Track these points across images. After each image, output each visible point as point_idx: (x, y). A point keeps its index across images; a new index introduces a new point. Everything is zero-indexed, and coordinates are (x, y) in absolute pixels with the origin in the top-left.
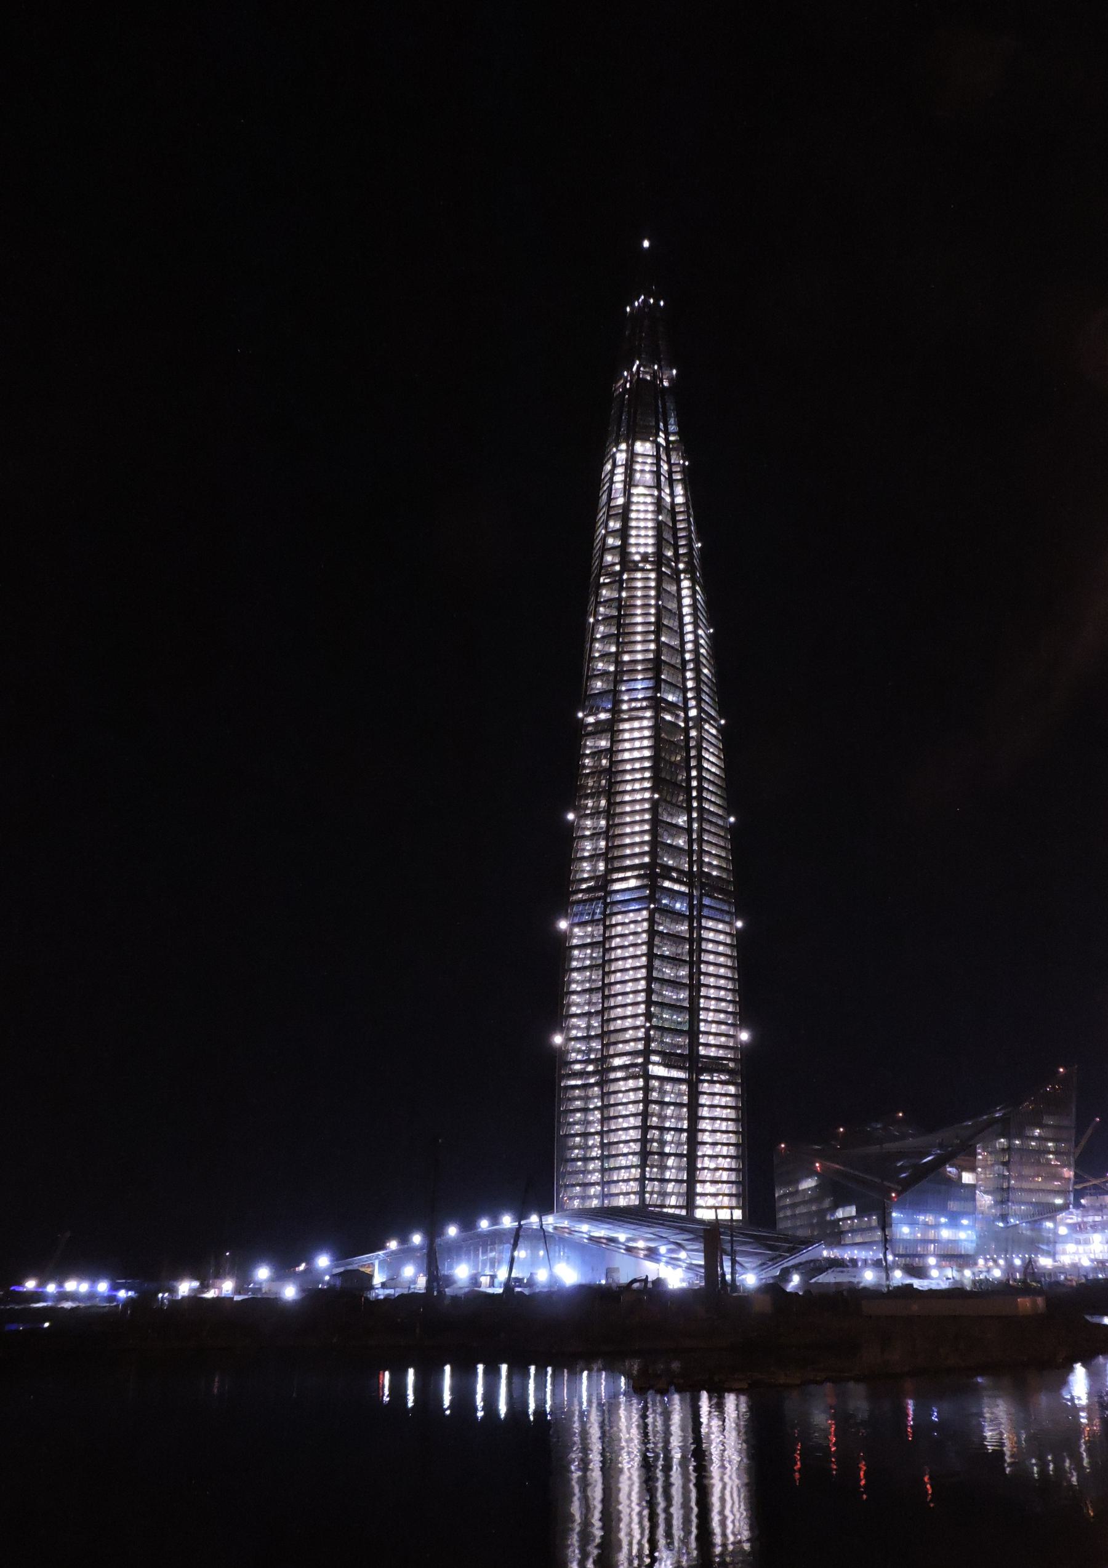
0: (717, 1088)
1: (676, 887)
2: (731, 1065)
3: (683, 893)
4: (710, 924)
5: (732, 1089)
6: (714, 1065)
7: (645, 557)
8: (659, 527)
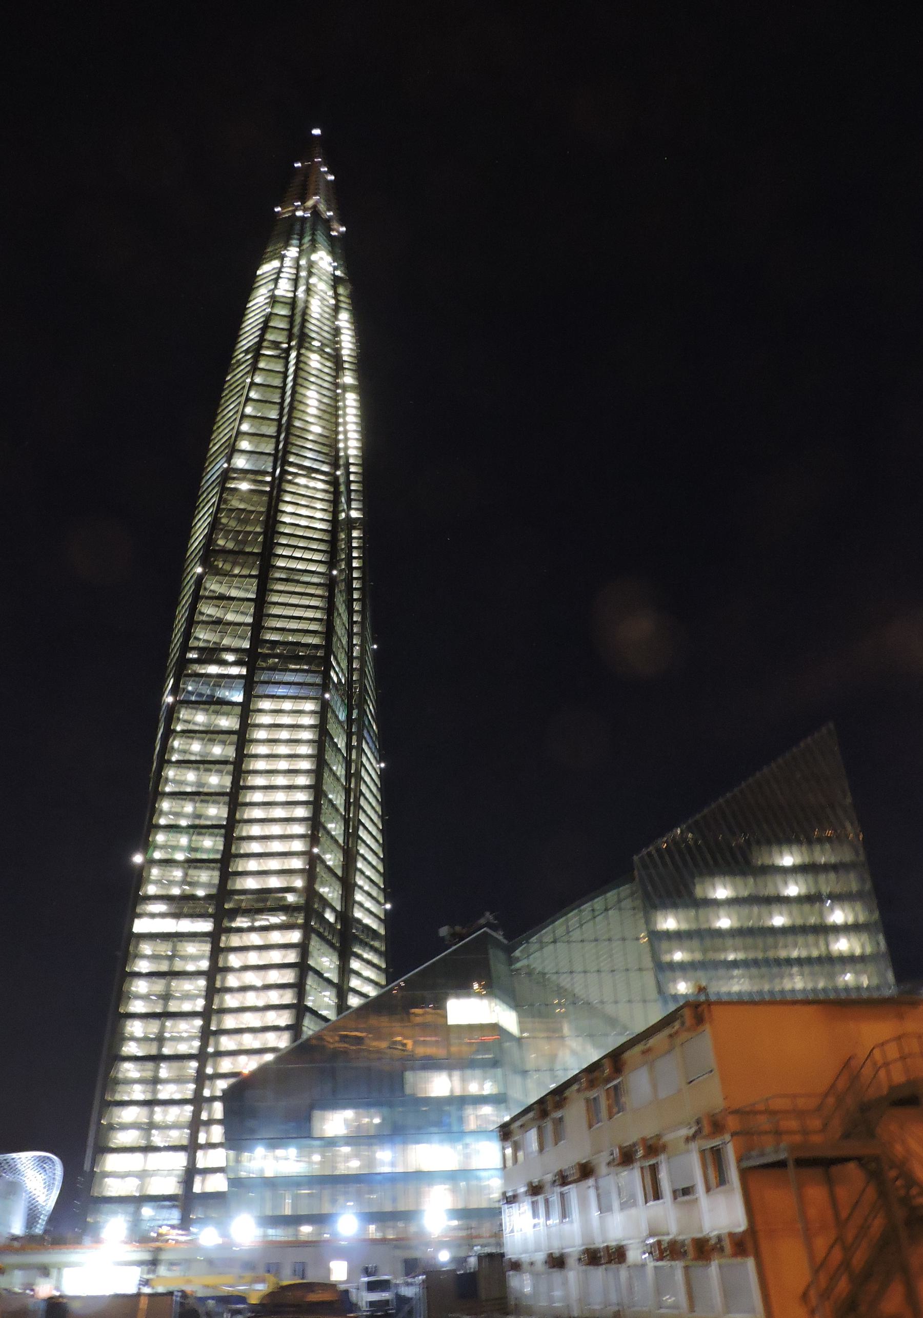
0: (276, 937)
1: (235, 671)
2: (291, 898)
3: (239, 676)
4: (287, 705)
5: (295, 936)
6: (265, 902)
7: (247, 352)
8: (268, 318)
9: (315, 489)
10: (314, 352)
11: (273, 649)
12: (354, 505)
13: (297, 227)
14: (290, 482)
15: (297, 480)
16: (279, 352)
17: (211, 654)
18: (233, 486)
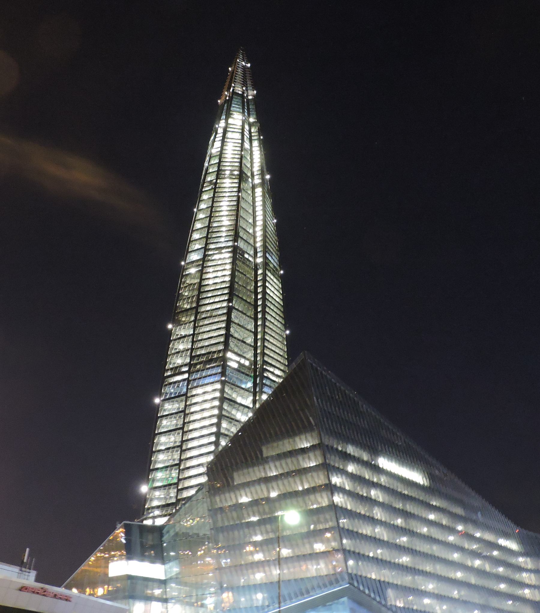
4: (209, 388)
9: (224, 258)
10: (224, 178)
11: (198, 359)
12: (259, 255)
13: (225, 108)
14: (209, 260)
15: (213, 258)
16: (212, 186)
17: (177, 371)
18: (187, 273)
